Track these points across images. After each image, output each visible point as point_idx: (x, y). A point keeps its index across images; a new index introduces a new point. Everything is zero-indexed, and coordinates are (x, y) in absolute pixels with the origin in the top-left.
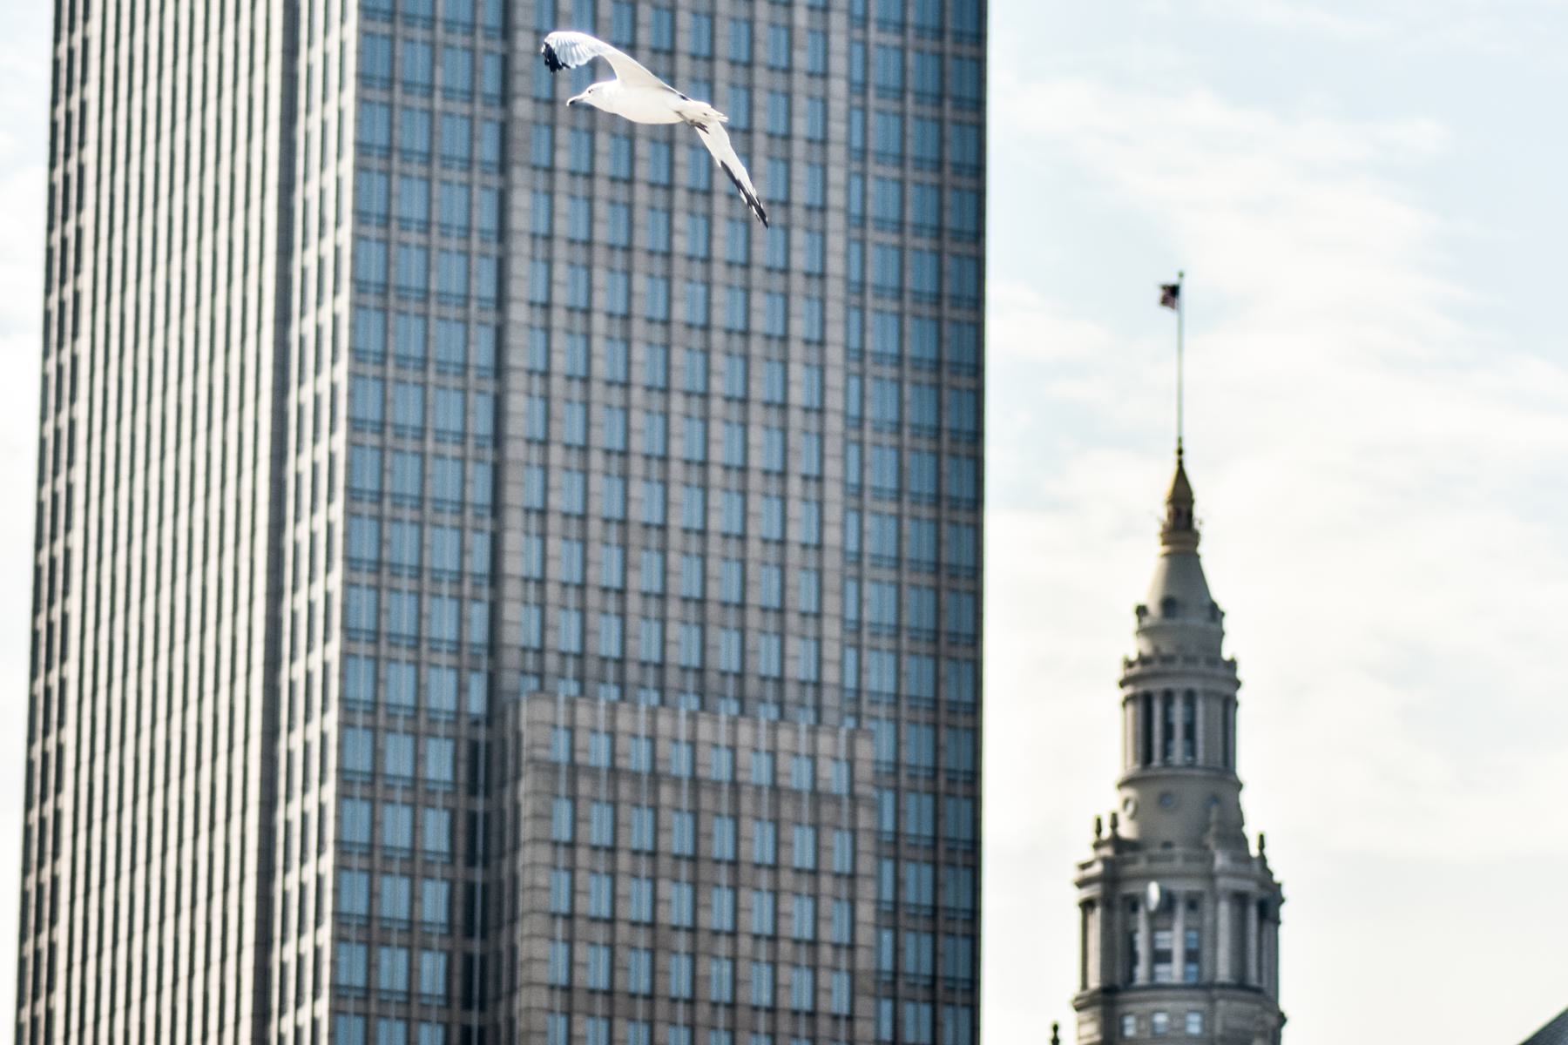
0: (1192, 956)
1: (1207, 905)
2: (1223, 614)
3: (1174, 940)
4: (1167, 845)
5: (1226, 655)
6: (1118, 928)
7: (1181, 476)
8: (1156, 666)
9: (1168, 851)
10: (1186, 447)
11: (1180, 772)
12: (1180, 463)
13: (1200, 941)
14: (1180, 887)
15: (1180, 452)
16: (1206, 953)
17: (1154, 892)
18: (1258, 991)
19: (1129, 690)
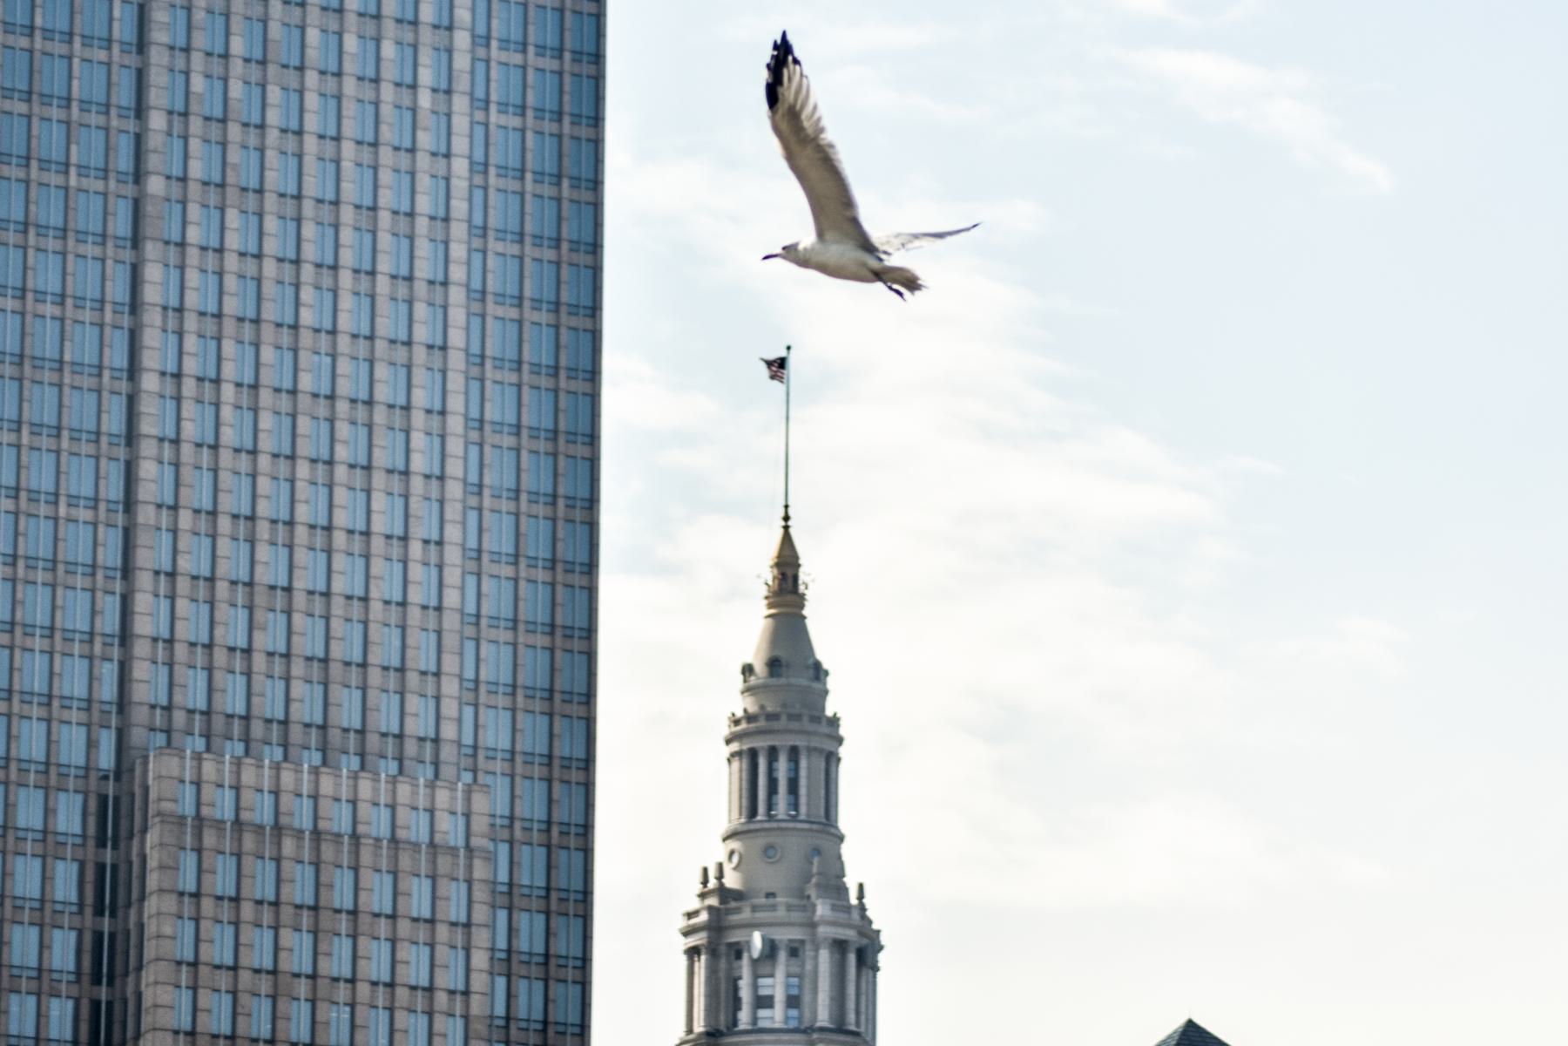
0: (793, 1002)
1: (808, 952)
2: (826, 673)
3: (776, 985)
4: (770, 895)
5: (829, 712)
6: (722, 974)
7: (787, 539)
8: (762, 723)
9: (771, 901)
10: (791, 512)
11: (783, 825)
12: (786, 528)
13: (800, 987)
14: (782, 935)
16: (807, 998)
17: (757, 939)
18: (856, 1034)
19: (735, 747)
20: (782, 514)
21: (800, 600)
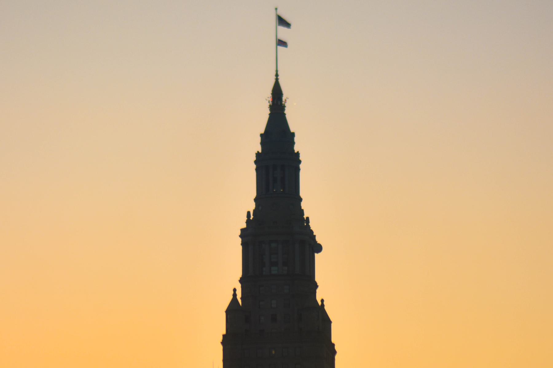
10: (279, 73)
15: (277, 75)
20: (275, 73)
21: (283, 108)
